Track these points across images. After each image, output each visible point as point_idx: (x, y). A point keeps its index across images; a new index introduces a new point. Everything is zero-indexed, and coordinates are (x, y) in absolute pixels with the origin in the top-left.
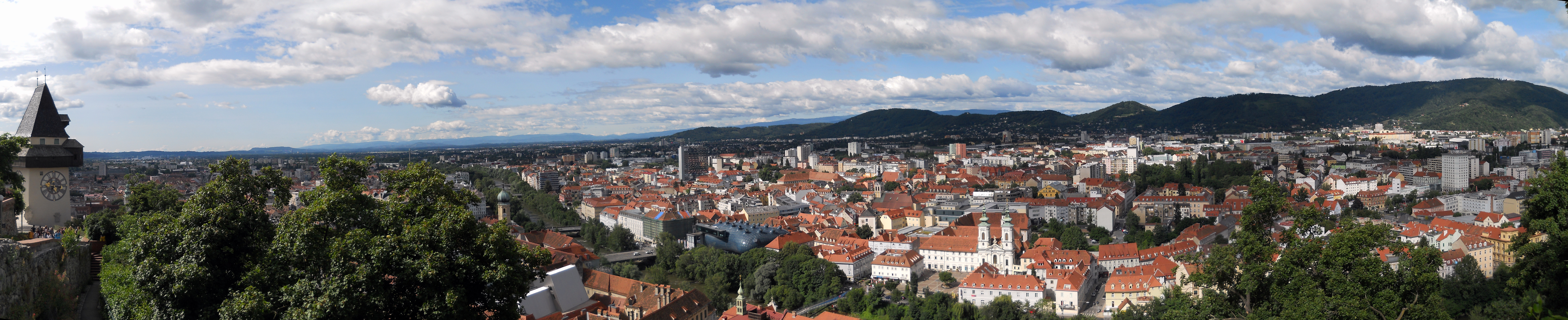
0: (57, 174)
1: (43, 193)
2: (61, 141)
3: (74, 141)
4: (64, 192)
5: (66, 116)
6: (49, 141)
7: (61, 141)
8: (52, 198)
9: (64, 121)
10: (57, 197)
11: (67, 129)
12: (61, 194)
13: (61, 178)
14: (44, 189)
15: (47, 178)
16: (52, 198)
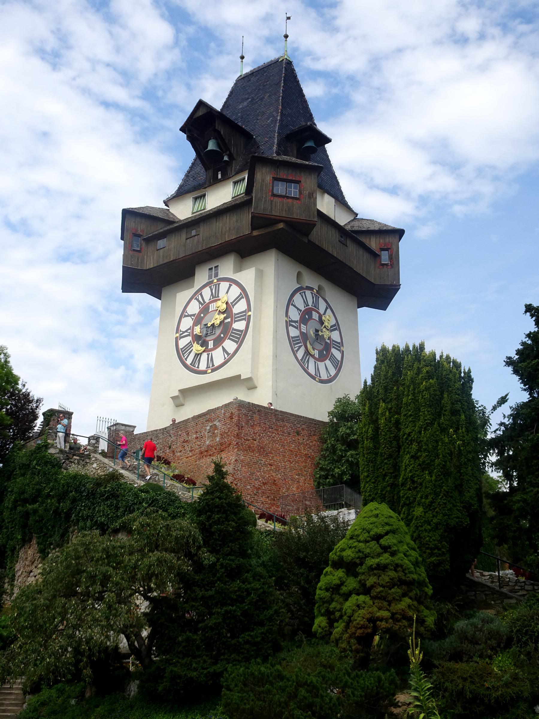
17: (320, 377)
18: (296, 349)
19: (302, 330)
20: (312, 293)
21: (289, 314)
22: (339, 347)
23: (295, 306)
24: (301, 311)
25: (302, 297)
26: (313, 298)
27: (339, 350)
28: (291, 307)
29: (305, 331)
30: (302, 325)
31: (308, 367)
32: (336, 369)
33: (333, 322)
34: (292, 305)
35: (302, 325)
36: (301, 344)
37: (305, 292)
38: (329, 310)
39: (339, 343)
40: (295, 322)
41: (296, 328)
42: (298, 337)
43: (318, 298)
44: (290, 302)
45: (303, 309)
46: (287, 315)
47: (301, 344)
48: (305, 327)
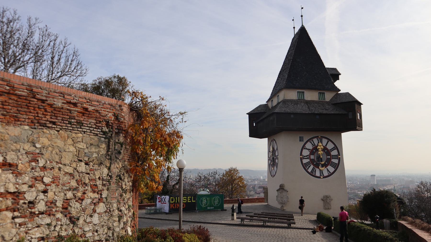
1: (305, 166)
2: (329, 96)
3: (348, 95)
4: (336, 166)
5: (335, 69)
6: (311, 96)
7: (329, 96)
8: (318, 174)
9: (335, 75)
10: (326, 173)
11: (337, 84)
12: (331, 169)
13: (330, 146)
14: (305, 161)
15: (309, 146)
16: (318, 174)
17: (323, 175)
21: (303, 154)
24: (310, 150)
25: (311, 143)
27: (337, 159)
28: (304, 150)
31: (315, 174)
33: (333, 146)
34: (305, 149)
37: (313, 141)
38: (330, 142)
39: (337, 155)
40: (306, 156)
41: (308, 158)
44: (303, 148)
45: (311, 148)
46: (301, 155)
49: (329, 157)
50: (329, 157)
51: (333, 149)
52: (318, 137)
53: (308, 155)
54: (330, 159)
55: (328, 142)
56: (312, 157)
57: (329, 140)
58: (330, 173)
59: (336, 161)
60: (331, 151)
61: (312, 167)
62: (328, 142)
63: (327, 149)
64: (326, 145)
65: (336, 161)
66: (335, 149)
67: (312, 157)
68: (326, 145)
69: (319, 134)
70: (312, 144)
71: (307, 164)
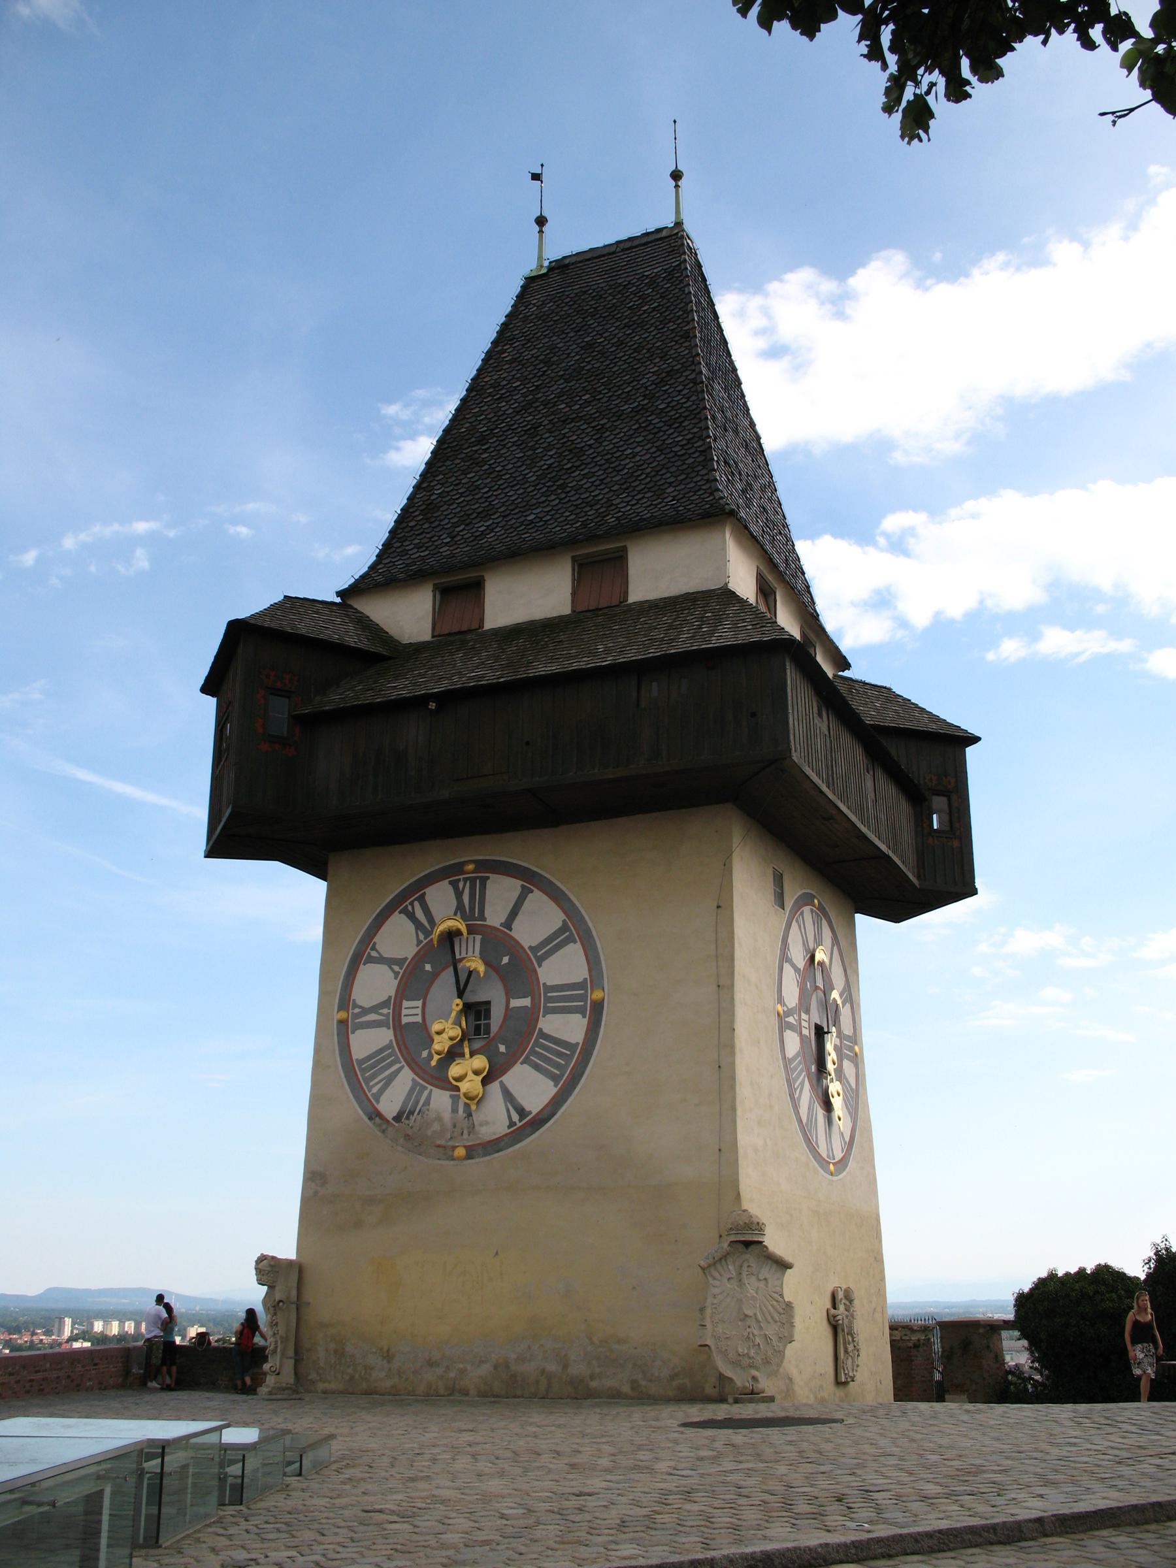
0: (501, 893)
14: (365, 1043)
15: (399, 938)
18: (375, 1090)
19: (405, 1020)
20: (455, 884)
22: (583, 998)
23: (381, 960)
24: (400, 962)
25: (412, 916)
26: (459, 895)
27: (581, 1011)
29: (419, 1019)
30: (405, 1004)
32: (555, 1079)
35: (405, 1004)
36: (397, 1066)
37: (422, 900)
38: (537, 898)
39: (581, 985)
40: (374, 1009)
42: (389, 1046)
43: (484, 881)
47: (397, 1066)
48: (419, 1003)
49: (526, 1002)
50: (526, 1002)
51: (553, 944)
52: (458, 869)
53: (385, 1004)
54: (530, 1017)
55: (525, 892)
56: (411, 1011)
57: (531, 879)
58: (522, 1112)
59: (569, 1027)
60: (540, 960)
61: (406, 1077)
62: (525, 892)
63: (513, 947)
64: (508, 924)
65: (569, 1027)
66: (570, 940)
67: (411, 1011)
68: (508, 924)
69: (469, 852)
70: (418, 925)
71: (378, 1059)
